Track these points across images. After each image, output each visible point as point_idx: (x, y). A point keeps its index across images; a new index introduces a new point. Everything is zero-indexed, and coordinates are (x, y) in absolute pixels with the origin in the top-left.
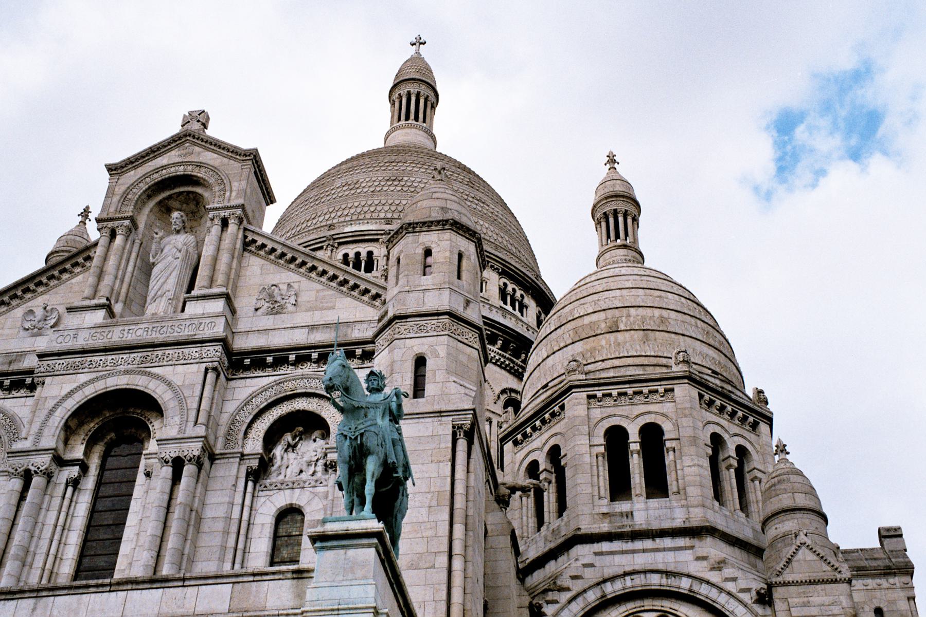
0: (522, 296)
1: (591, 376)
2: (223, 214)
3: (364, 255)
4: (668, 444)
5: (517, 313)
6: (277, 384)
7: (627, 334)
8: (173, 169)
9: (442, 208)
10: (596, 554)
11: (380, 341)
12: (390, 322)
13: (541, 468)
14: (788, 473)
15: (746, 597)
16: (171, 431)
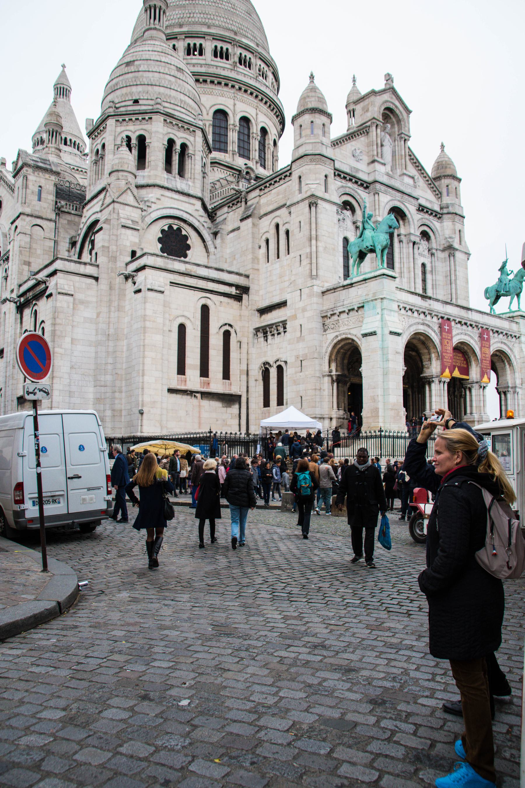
2: (406, 138)
11: (444, 216)
12: (453, 213)
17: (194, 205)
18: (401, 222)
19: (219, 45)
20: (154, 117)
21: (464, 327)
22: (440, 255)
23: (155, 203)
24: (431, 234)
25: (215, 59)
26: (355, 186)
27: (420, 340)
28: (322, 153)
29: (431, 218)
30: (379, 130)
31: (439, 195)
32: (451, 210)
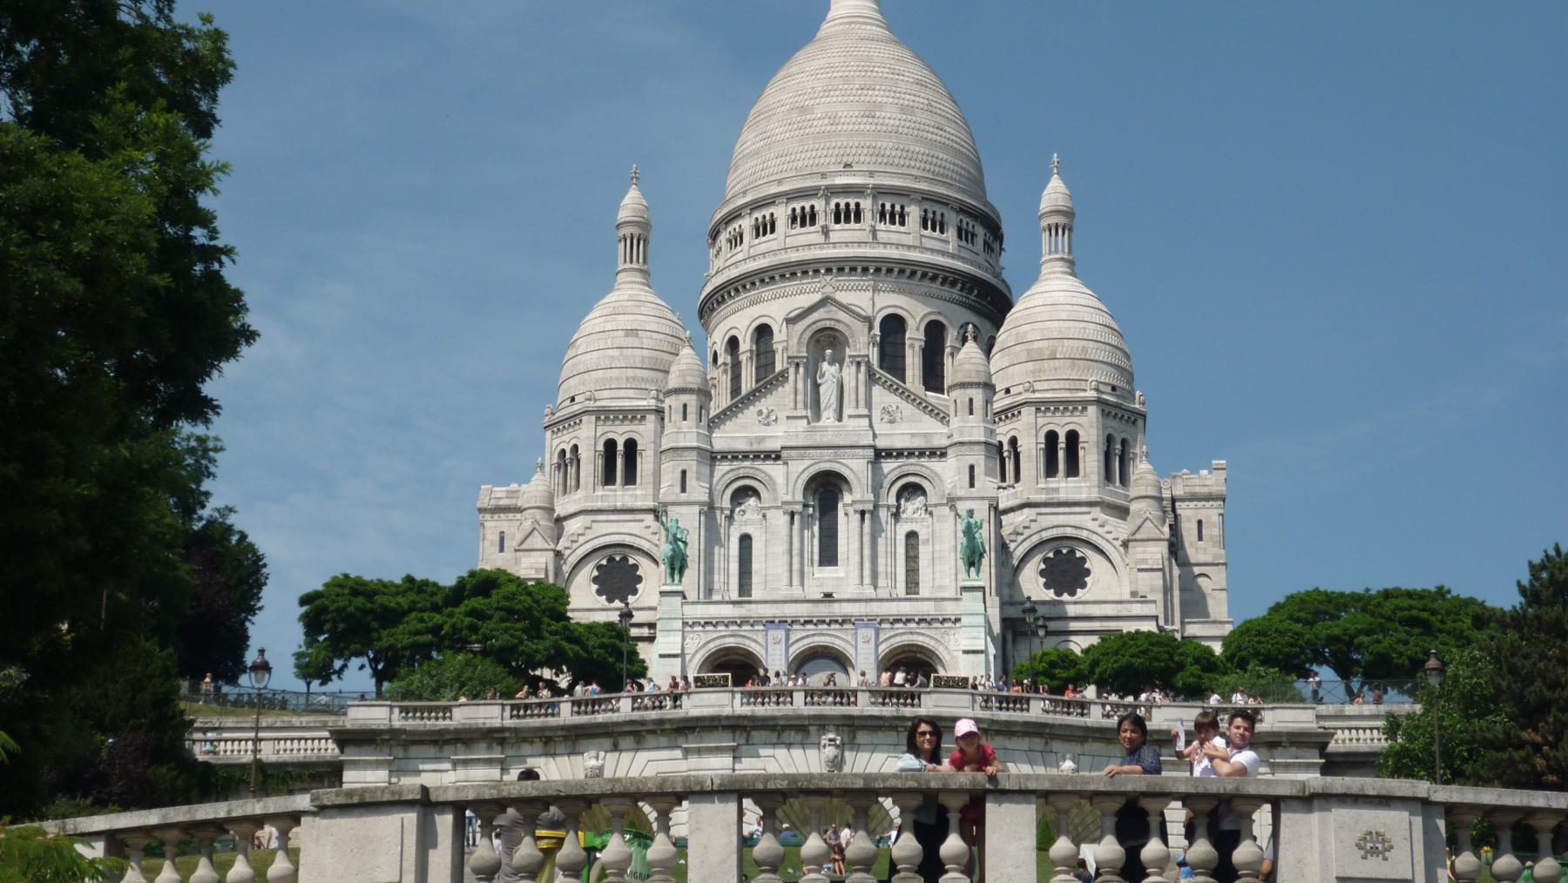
0: (973, 227)
1: (1038, 395)
3: (852, 207)
4: (1081, 445)
5: (970, 246)
6: (900, 467)
7: (1062, 361)
8: (823, 323)
9: (977, 371)
10: (1038, 514)
11: (950, 451)
12: (956, 444)
13: (1006, 447)
14: (1145, 473)
15: (1115, 542)
16: (857, 495)
17: (642, 521)
18: (845, 487)
19: (798, 205)
20: (585, 418)
21: (820, 627)
22: (947, 509)
23: (583, 535)
24: (925, 484)
25: (794, 232)
26: (758, 464)
27: (737, 654)
28: (674, 445)
29: (923, 460)
30: (801, 370)
31: (943, 418)
32: (956, 439)
